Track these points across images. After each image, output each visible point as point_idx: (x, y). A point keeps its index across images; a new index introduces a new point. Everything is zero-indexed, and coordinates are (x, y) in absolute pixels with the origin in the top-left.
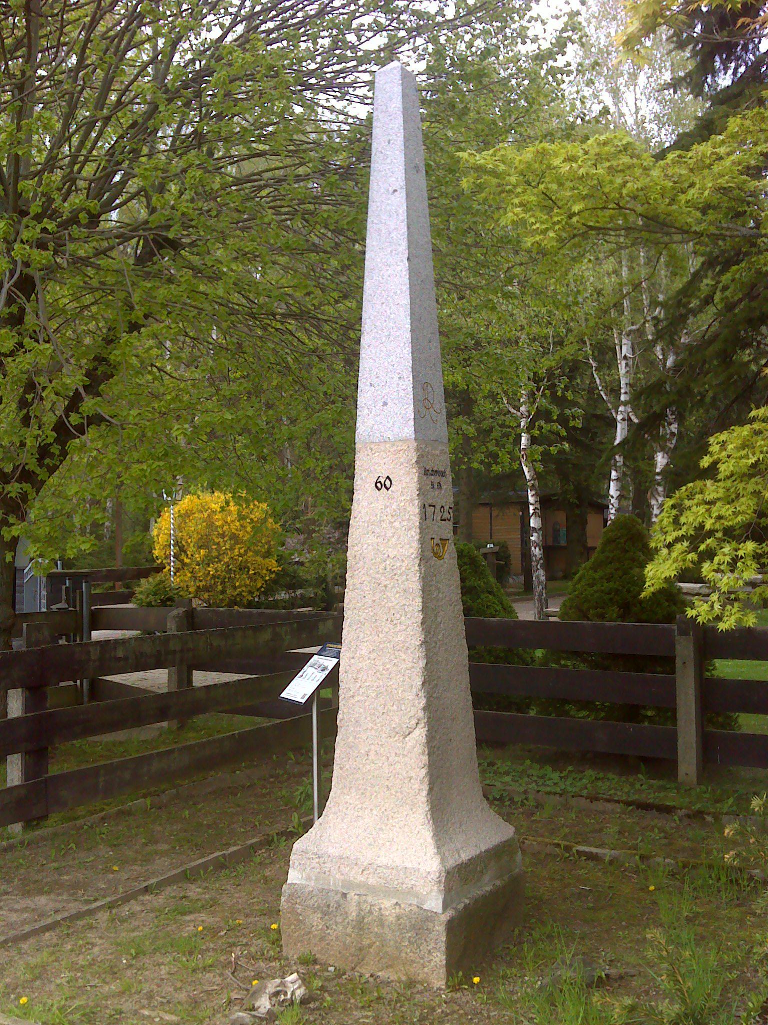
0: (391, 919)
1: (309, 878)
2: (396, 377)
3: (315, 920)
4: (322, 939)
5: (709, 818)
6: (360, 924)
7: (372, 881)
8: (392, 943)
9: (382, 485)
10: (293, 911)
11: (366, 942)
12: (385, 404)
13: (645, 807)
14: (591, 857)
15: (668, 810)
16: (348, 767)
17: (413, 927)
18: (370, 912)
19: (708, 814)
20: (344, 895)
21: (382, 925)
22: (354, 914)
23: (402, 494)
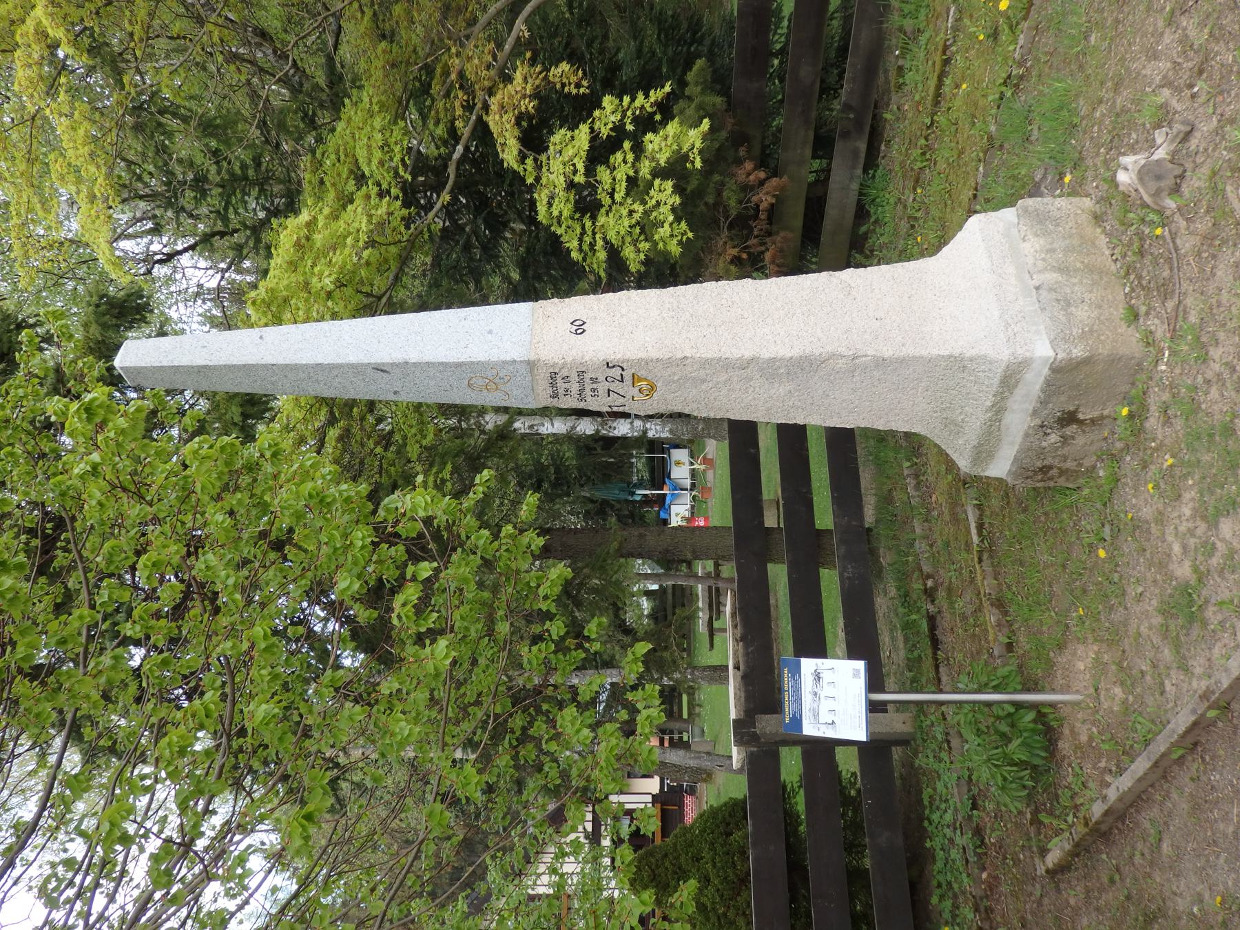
0: (1042, 242)
1: (1038, 332)
2: (463, 322)
3: (1083, 314)
4: (1100, 307)
5: (930, 583)
6: (1063, 269)
7: (1011, 270)
8: (1067, 242)
9: (579, 328)
10: (1083, 336)
11: (1078, 265)
12: (490, 332)
13: (935, 643)
14: (980, 527)
15: (932, 620)
16: (899, 338)
17: (1040, 222)
18: (1044, 260)
19: (926, 585)
20: (1037, 288)
21: (1052, 251)
22: (1055, 275)
23: (591, 309)
